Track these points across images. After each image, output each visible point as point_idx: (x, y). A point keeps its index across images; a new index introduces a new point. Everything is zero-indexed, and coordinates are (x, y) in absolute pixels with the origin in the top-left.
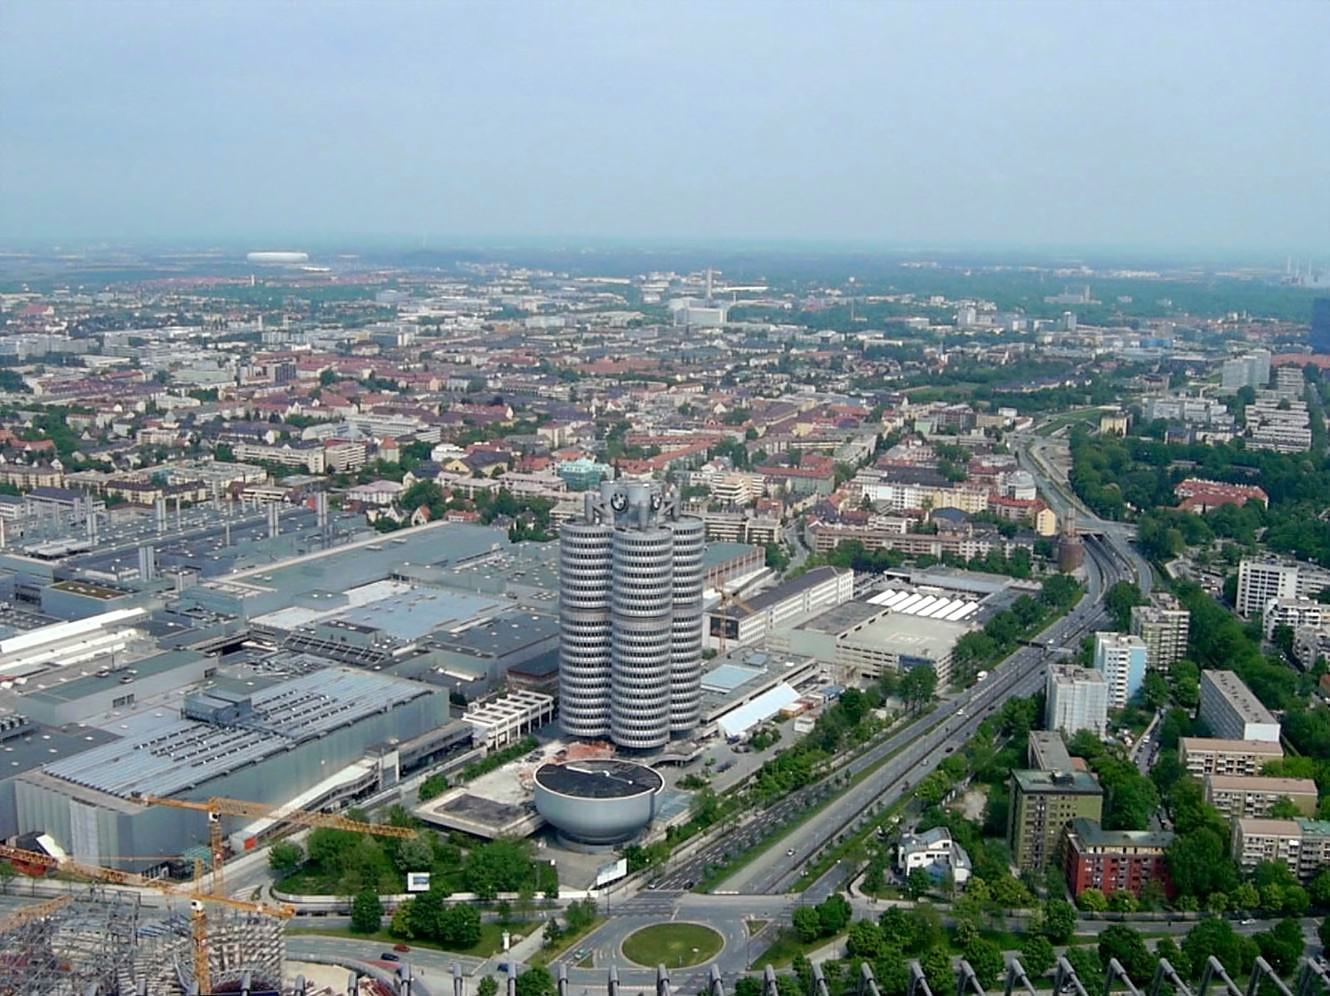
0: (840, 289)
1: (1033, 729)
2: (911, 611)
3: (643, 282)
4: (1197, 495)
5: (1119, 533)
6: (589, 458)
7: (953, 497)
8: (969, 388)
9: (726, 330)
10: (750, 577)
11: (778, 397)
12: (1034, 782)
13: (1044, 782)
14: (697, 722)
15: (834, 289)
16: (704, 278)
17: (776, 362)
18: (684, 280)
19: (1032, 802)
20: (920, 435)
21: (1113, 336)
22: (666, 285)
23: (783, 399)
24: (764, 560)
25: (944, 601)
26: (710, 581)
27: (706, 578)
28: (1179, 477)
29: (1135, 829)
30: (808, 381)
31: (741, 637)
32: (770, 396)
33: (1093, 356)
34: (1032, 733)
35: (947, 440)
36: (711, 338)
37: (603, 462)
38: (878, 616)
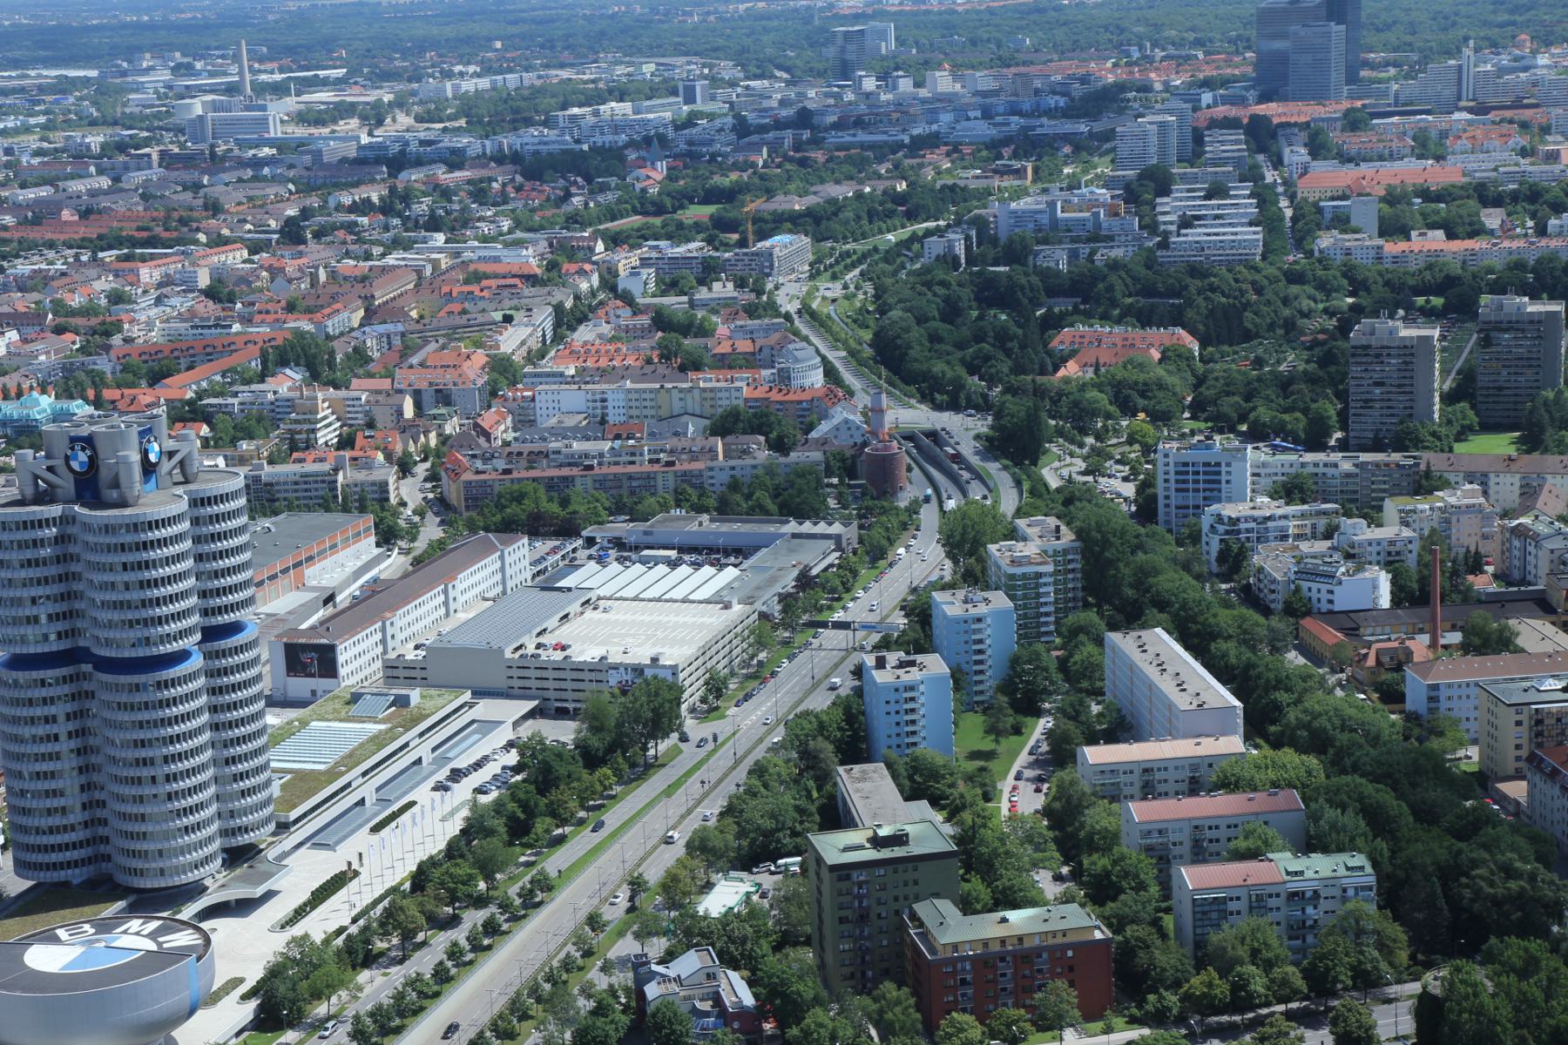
0: (476, 64)
1: (842, 763)
2: (629, 592)
3: (124, 74)
4: (1088, 352)
5: (964, 430)
6: (44, 392)
7: (689, 396)
8: (700, 212)
9: (281, 145)
10: (353, 565)
11: (383, 255)
12: (846, 849)
13: (861, 847)
14: (272, 827)
15: (469, 63)
16: (236, 58)
17: (375, 198)
18: (199, 65)
19: (844, 885)
20: (627, 299)
21: (938, 105)
22: (164, 75)
23: (391, 260)
24: (373, 539)
25: (684, 570)
26: (283, 581)
27: (272, 578)
28: (1054, 323)
29: (1015, 906)
30: (434, 224)
31: (342, 672)
32: (368, 256)
33: (907, 141)
34: (841, 769)
35: (674, 302)
36: (257, 163)
37: (71, 397)
38: (575, 608)
